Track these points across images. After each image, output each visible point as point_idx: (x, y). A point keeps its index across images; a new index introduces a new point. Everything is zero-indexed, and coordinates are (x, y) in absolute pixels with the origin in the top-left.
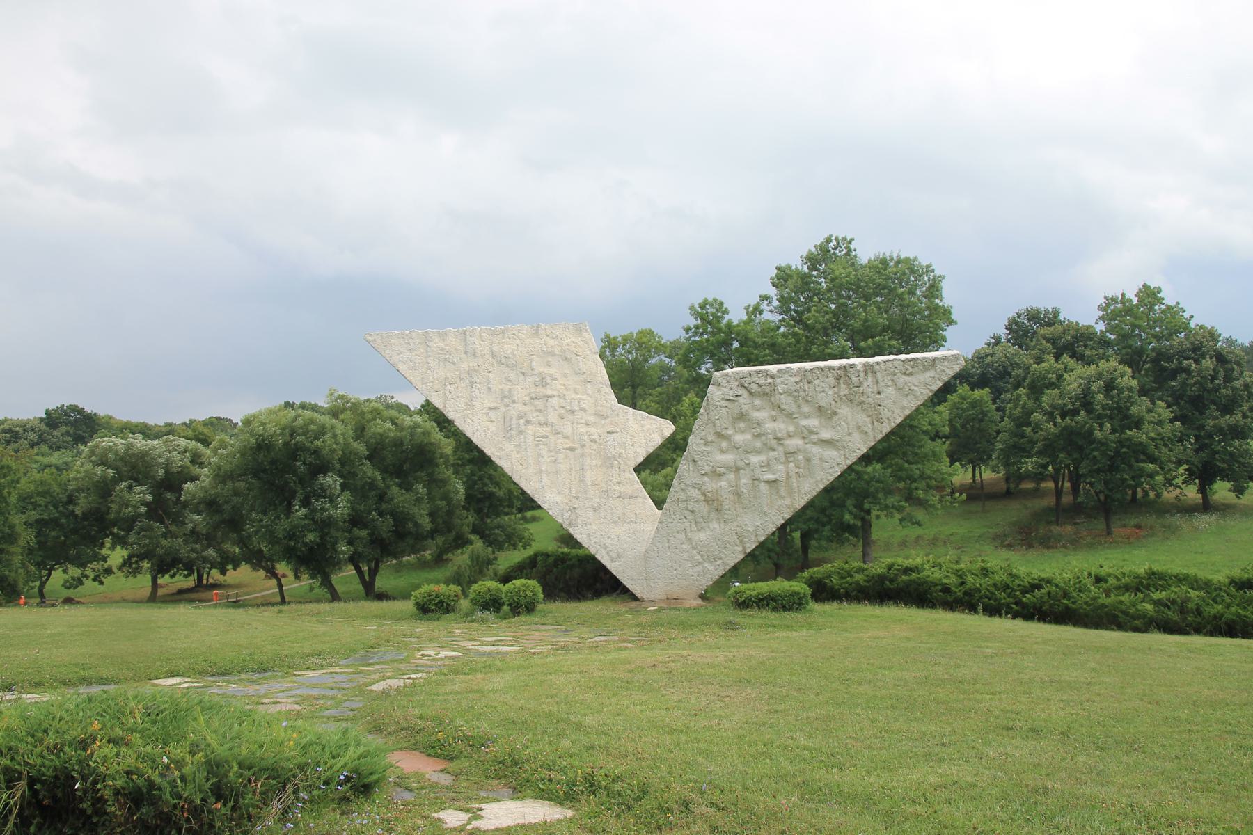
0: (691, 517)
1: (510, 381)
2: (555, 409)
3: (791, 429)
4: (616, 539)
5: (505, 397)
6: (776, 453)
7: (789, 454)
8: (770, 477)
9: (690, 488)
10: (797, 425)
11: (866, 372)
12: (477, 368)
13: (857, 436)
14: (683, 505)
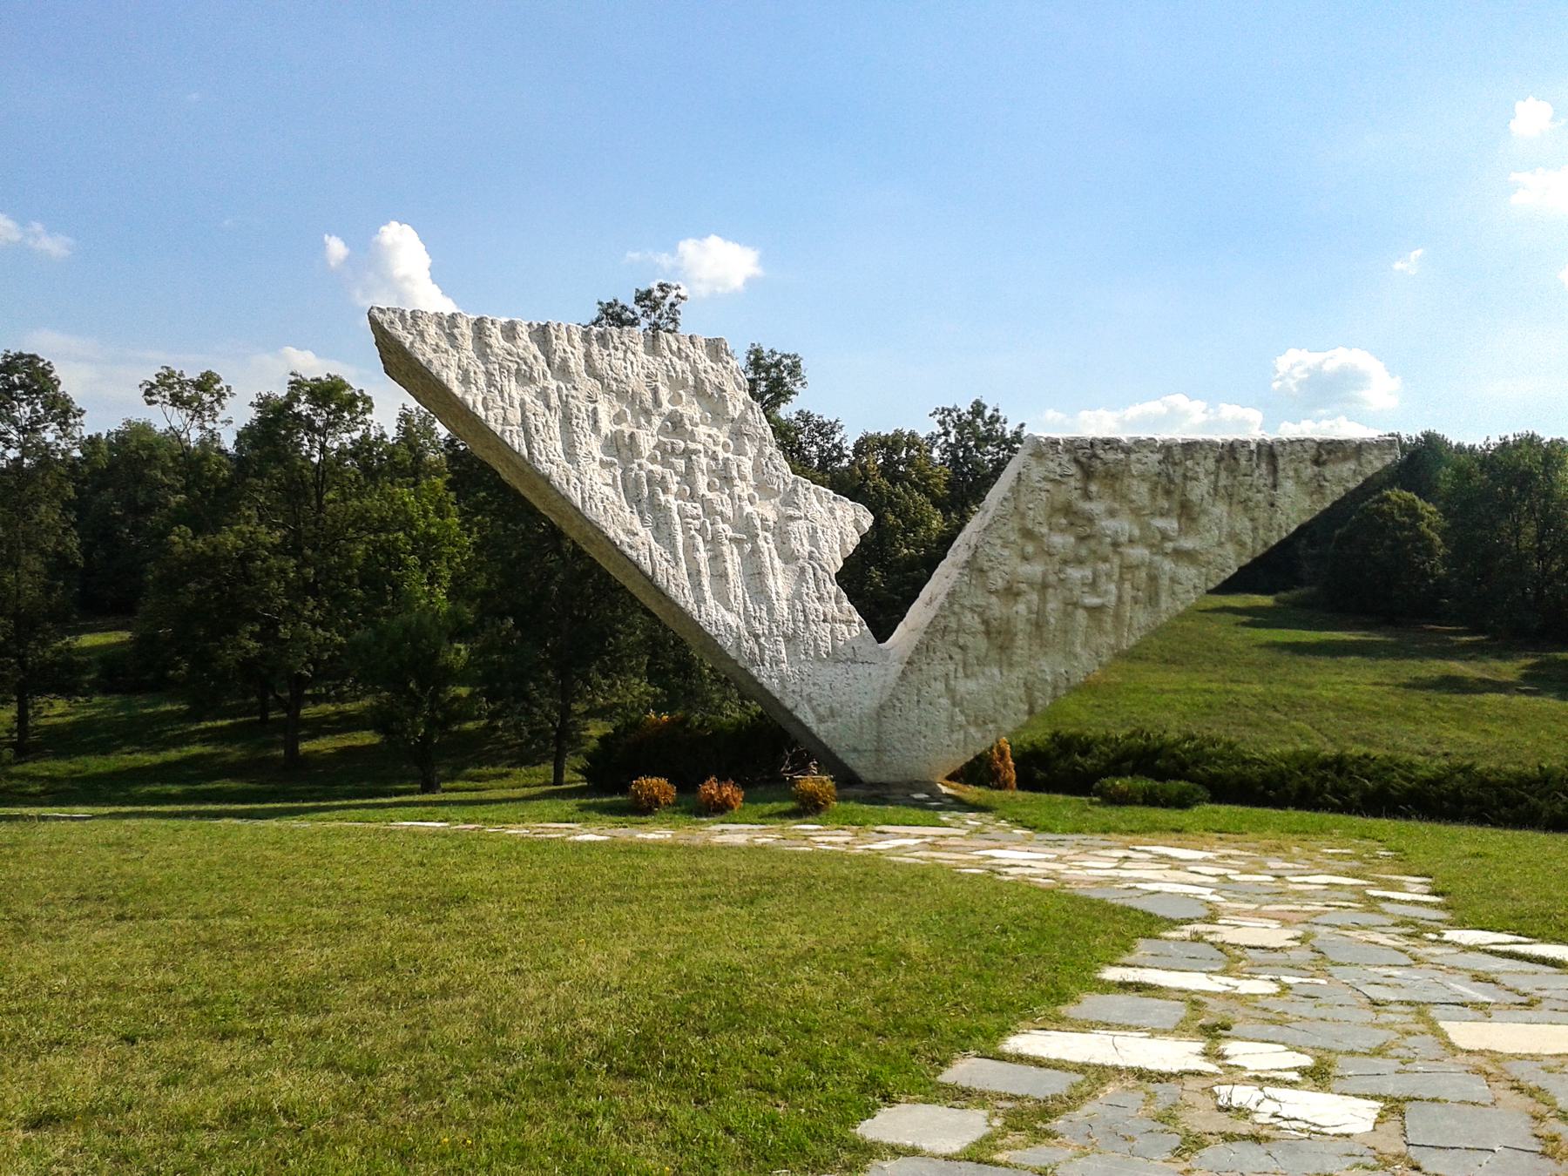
0: (958, 657)
3: (1137, 532)
4: (827, 687)
6: (1108, 565)
7: (1128, 568)
9: (967, 612)
10: (1145, 527)
11: (1259, 453)
13: (1230, 548)
14: (952, 637)
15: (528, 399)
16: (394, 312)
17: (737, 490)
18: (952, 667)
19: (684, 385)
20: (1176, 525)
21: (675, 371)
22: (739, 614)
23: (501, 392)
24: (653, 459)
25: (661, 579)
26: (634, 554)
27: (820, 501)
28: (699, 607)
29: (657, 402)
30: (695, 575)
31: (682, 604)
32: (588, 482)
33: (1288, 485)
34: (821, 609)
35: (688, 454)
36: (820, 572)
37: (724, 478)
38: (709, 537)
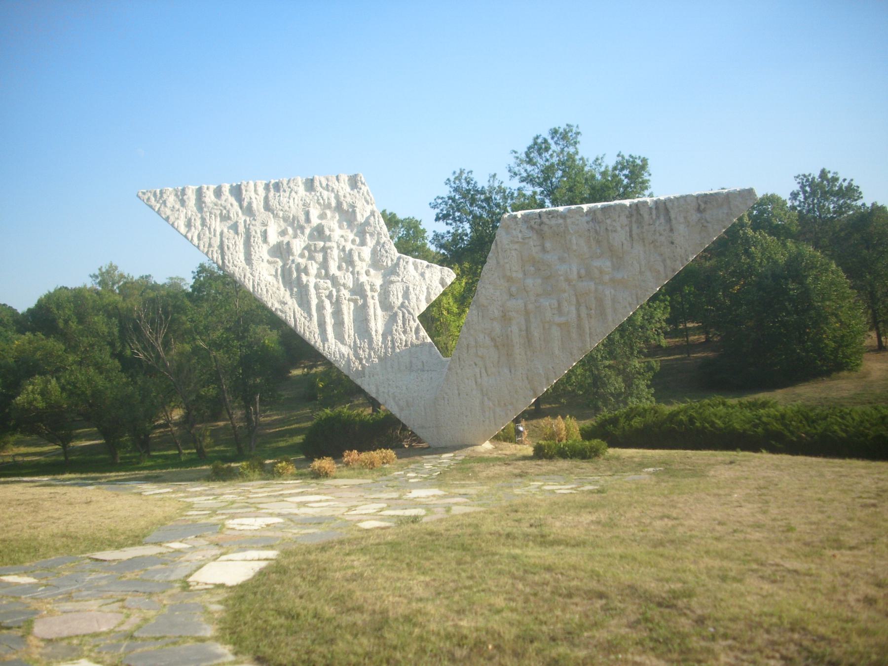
4: (404, 388)
8: (563, 319)
15: (225, 230)
16: (150, 192)
17: (357, 269)
18: (477, 370)
19: (329, 206)
20: (608, 264)
21: (323, 199)
22: (350, 346)
23: (209, 229)
24: (302, 256)
25: (300, 330)
26: (283, 315)
27: (416, 268)
28: (324, 344)
29: (308, 220)
30: (322, 325)
31: (313, 343)
32: (257, 275)
33: (681, 229)
34: (404, 338)
35: (324, 250)
36: (407, 315)
37: (348, 260)
38: (334, 300)
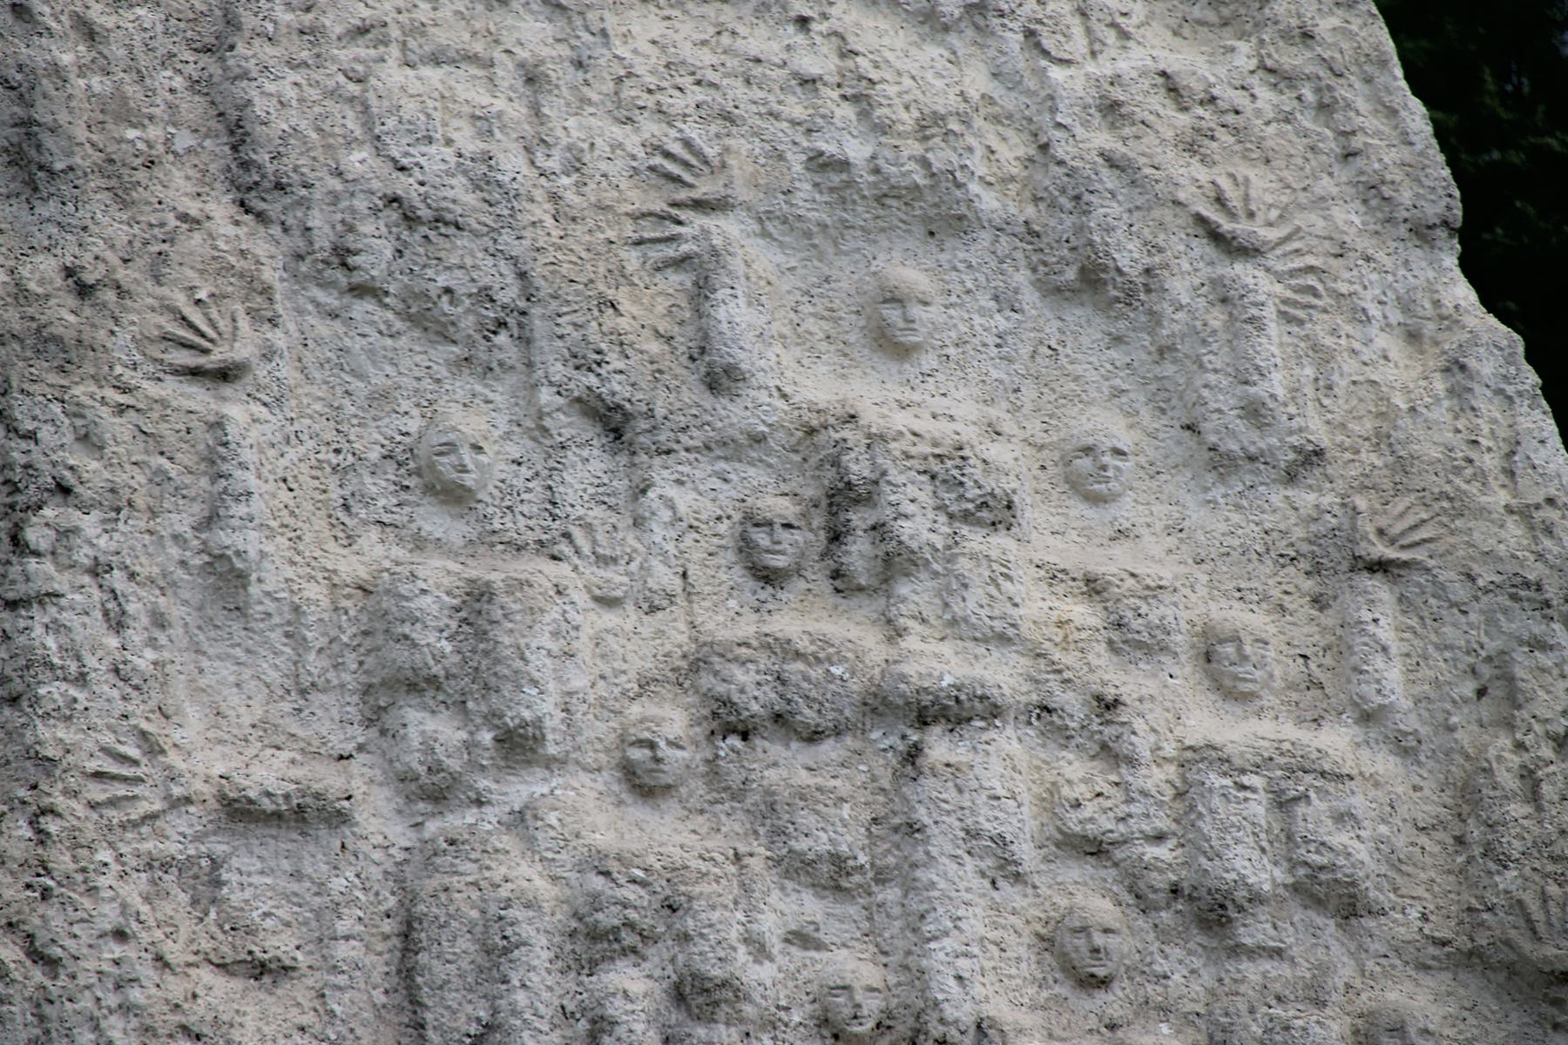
1: (454, 496)
2: (1007, 870)
5: (418, 684)
12: (64, 314)
